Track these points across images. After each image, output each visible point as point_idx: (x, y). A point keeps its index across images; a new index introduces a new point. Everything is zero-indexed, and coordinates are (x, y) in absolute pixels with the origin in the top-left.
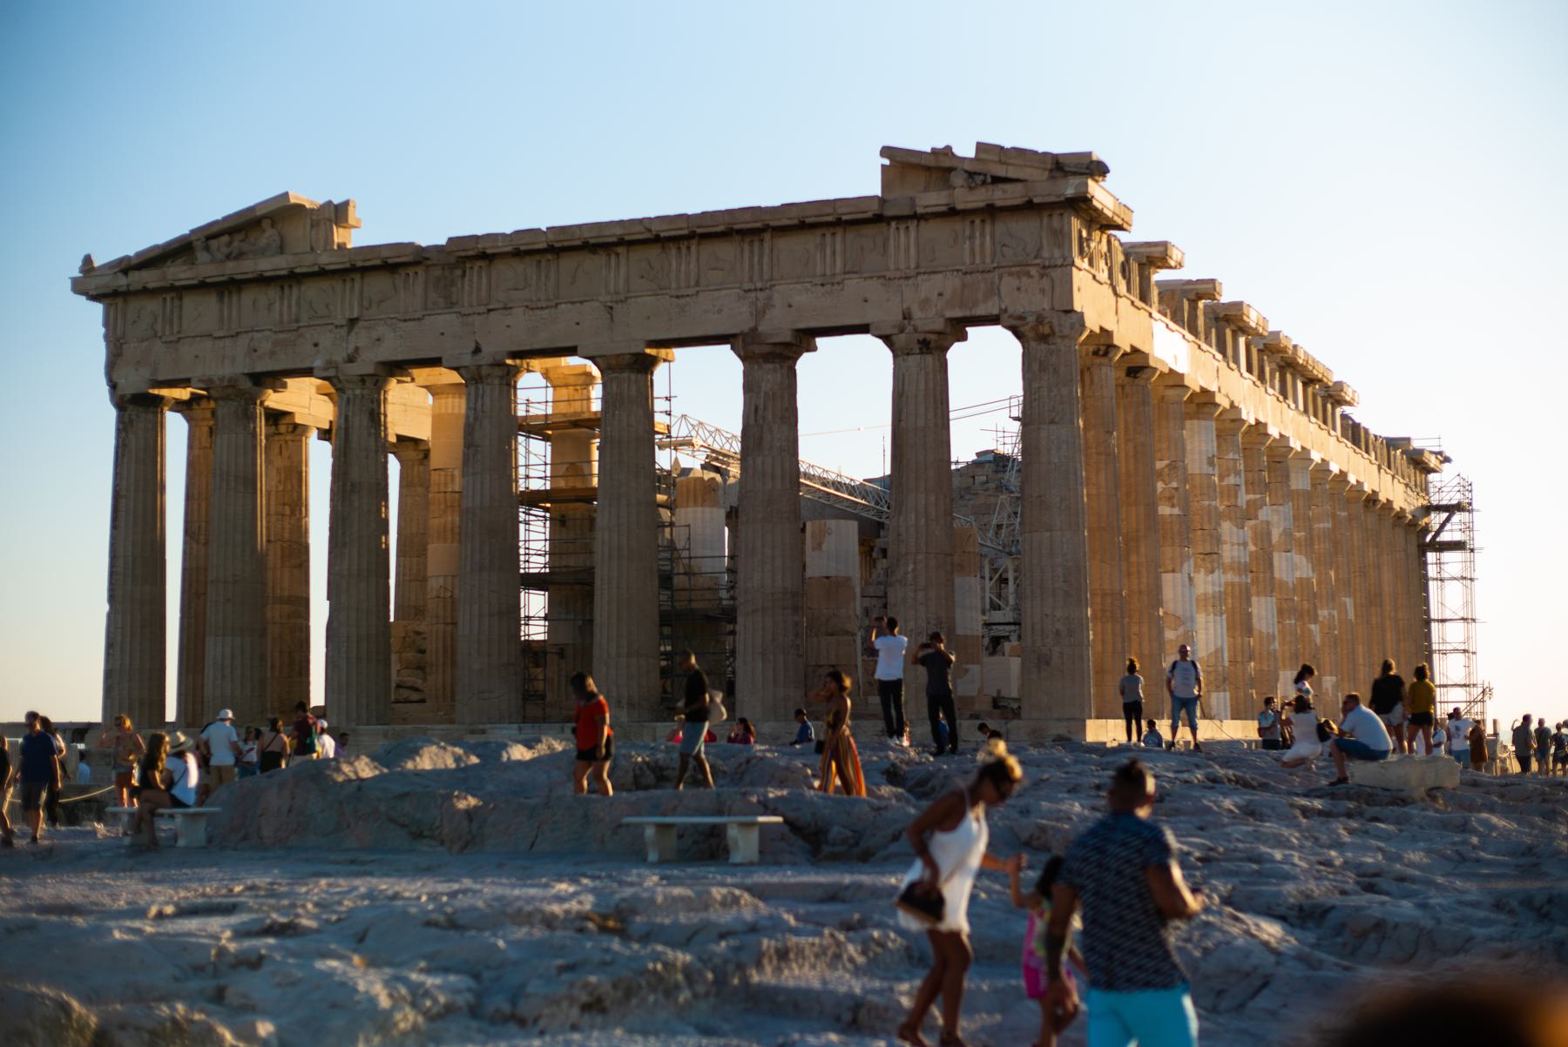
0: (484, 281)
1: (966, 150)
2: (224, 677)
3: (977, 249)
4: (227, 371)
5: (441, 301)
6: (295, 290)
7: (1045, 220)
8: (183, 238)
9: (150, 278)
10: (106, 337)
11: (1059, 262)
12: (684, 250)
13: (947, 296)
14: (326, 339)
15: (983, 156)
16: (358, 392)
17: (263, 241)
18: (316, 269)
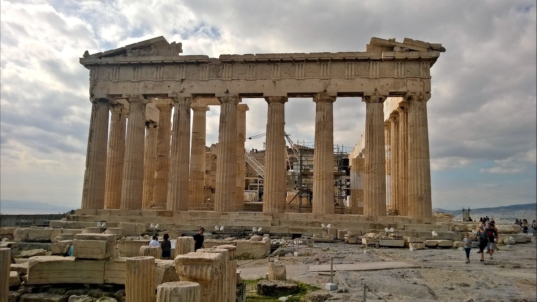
0: (230, 70)
1: (400, 40)
2: (130, 193)
3: (399, 72)
4: (136, 93)
5: (215, 76)
6: (162, 69)
7: (422, 65)
8: (123, 48)
9: (110, 60)
10: (90, 79)
11: (427, 77)
12: (300, 65)
13: (390, 84)
14: (173, 85)
15: (406, 42)
16: (183, 103)
17: (152, 52)
18: (172, 61)
